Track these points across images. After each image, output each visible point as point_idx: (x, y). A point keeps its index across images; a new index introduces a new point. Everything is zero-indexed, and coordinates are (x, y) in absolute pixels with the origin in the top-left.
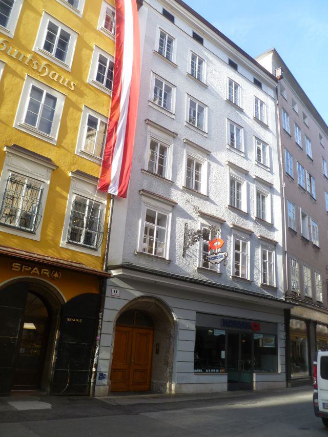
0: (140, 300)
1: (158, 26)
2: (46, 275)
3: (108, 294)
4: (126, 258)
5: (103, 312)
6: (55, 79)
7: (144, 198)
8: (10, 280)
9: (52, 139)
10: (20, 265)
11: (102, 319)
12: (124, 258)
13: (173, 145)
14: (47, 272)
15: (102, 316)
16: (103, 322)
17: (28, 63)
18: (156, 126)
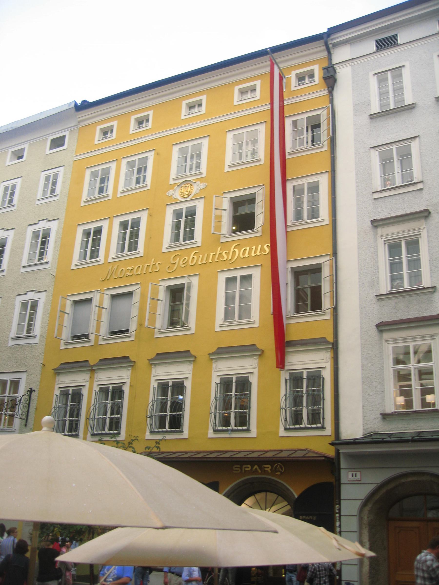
0: (403, 481)
1: (371, 74)
2: (267, 471)
3: (343, 479)
4: (370, 426)
5: (340, 504)
6: (246, 255)
7: (386, 336)
8: (237, 482)
9: (253, 322)
10: (239, 466)
11: (340, 513)
12: (365, 428)
13: (425, 231)
14: (268, 468)
15: (340, 510)
16: (342, 517)
17: (218, 259)
18: (388, 221)
